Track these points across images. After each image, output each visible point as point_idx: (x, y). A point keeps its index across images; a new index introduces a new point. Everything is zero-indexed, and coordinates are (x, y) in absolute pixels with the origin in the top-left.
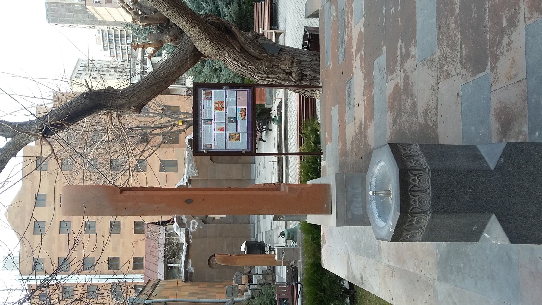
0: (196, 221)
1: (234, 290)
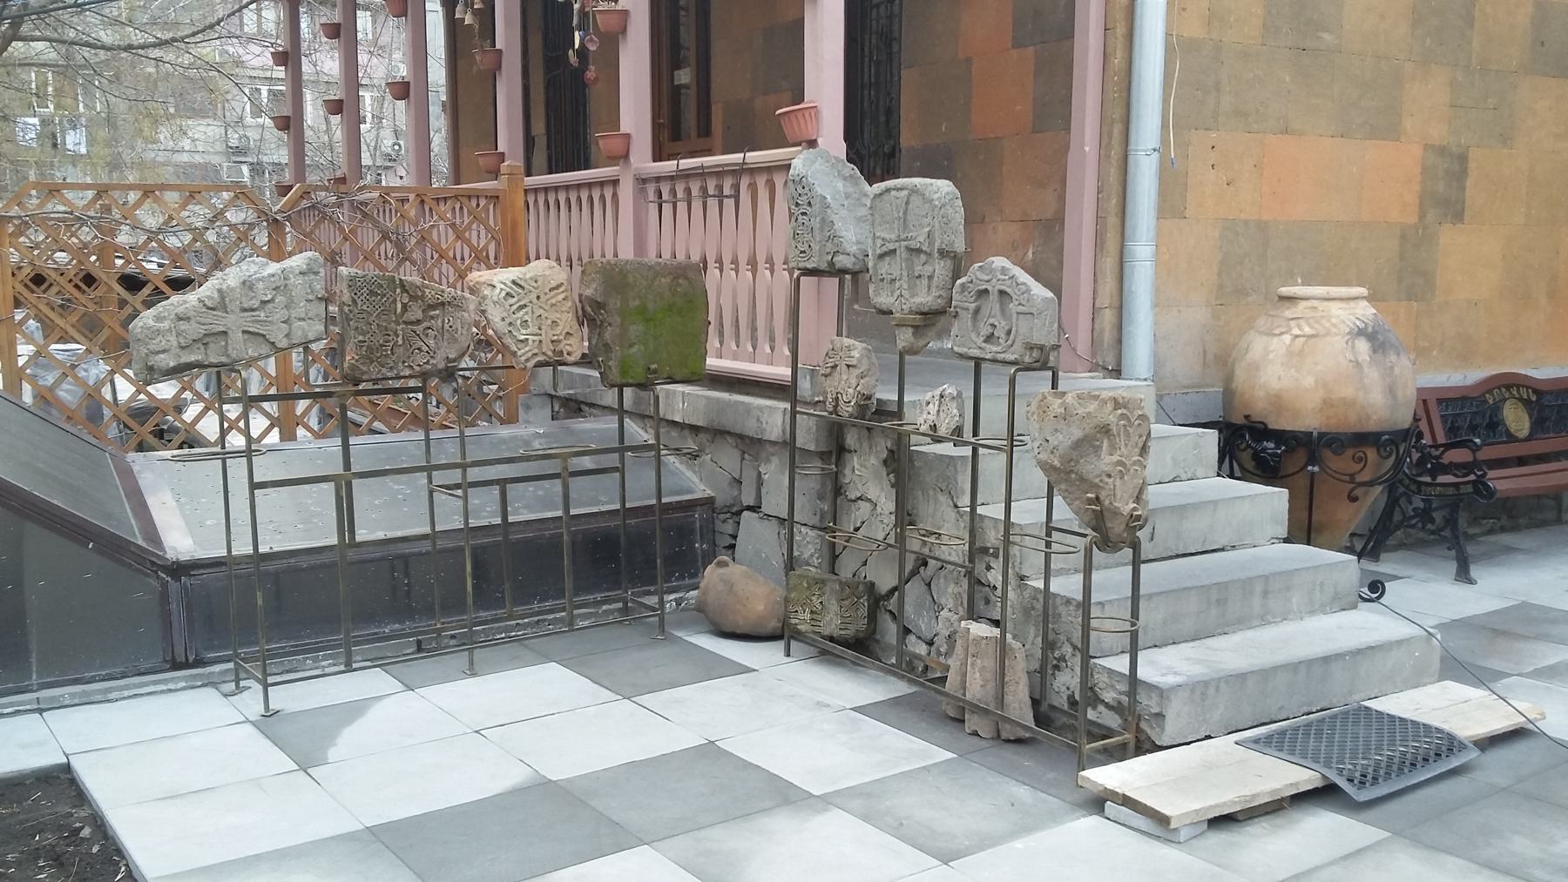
1: (918, 269)
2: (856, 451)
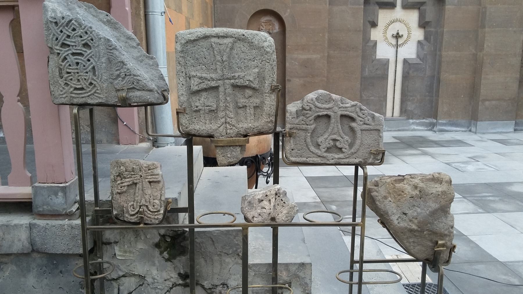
1: (242, 101)
2: (116, 243)
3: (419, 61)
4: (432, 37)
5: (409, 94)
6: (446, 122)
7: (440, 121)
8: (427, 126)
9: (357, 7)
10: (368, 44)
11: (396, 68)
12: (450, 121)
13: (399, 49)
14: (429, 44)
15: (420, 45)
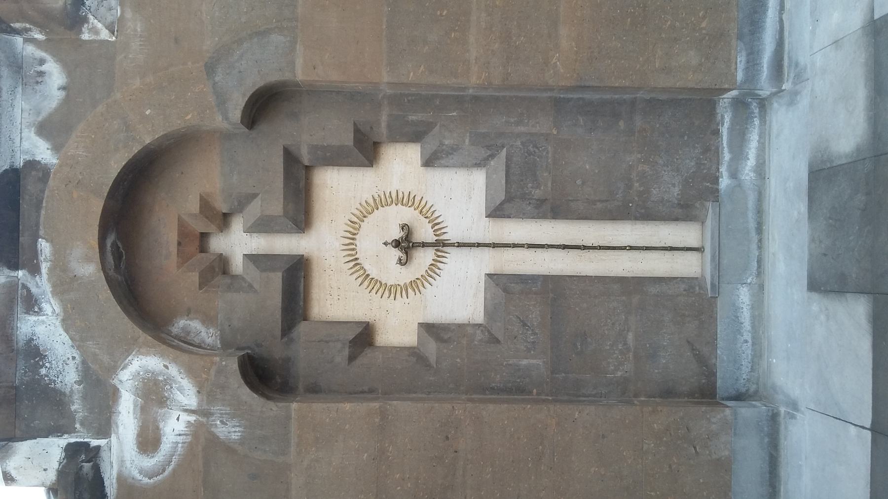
0: (174, 371)
3: (499, 162)
4: (412, 118)
5: (619, 196)
6: (744, 53)
7: (740, 76)
8: (749, 118)
9: (293, 427)
10: (433, 359)
11: (521, 246)
12: (740, 37)
13: (452, 234)
14: (437, 128)
15: (438, 158)
